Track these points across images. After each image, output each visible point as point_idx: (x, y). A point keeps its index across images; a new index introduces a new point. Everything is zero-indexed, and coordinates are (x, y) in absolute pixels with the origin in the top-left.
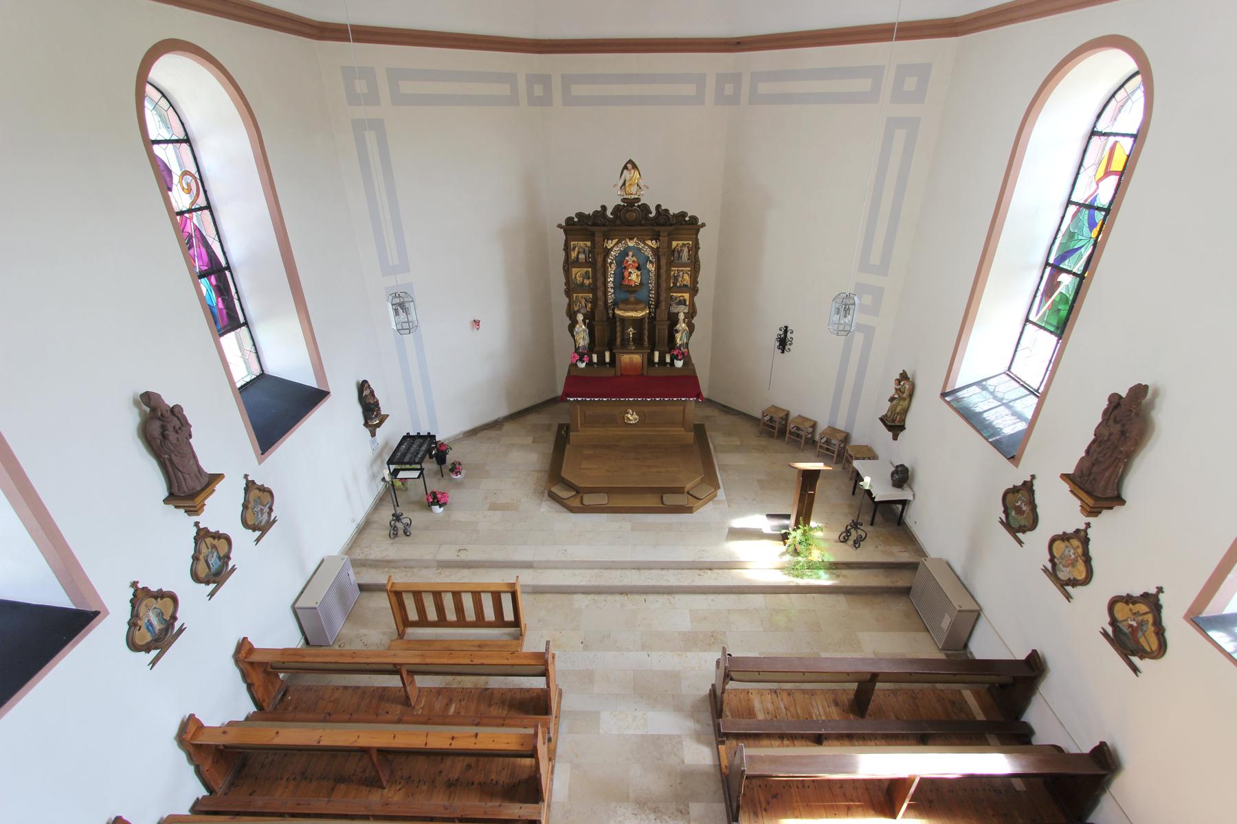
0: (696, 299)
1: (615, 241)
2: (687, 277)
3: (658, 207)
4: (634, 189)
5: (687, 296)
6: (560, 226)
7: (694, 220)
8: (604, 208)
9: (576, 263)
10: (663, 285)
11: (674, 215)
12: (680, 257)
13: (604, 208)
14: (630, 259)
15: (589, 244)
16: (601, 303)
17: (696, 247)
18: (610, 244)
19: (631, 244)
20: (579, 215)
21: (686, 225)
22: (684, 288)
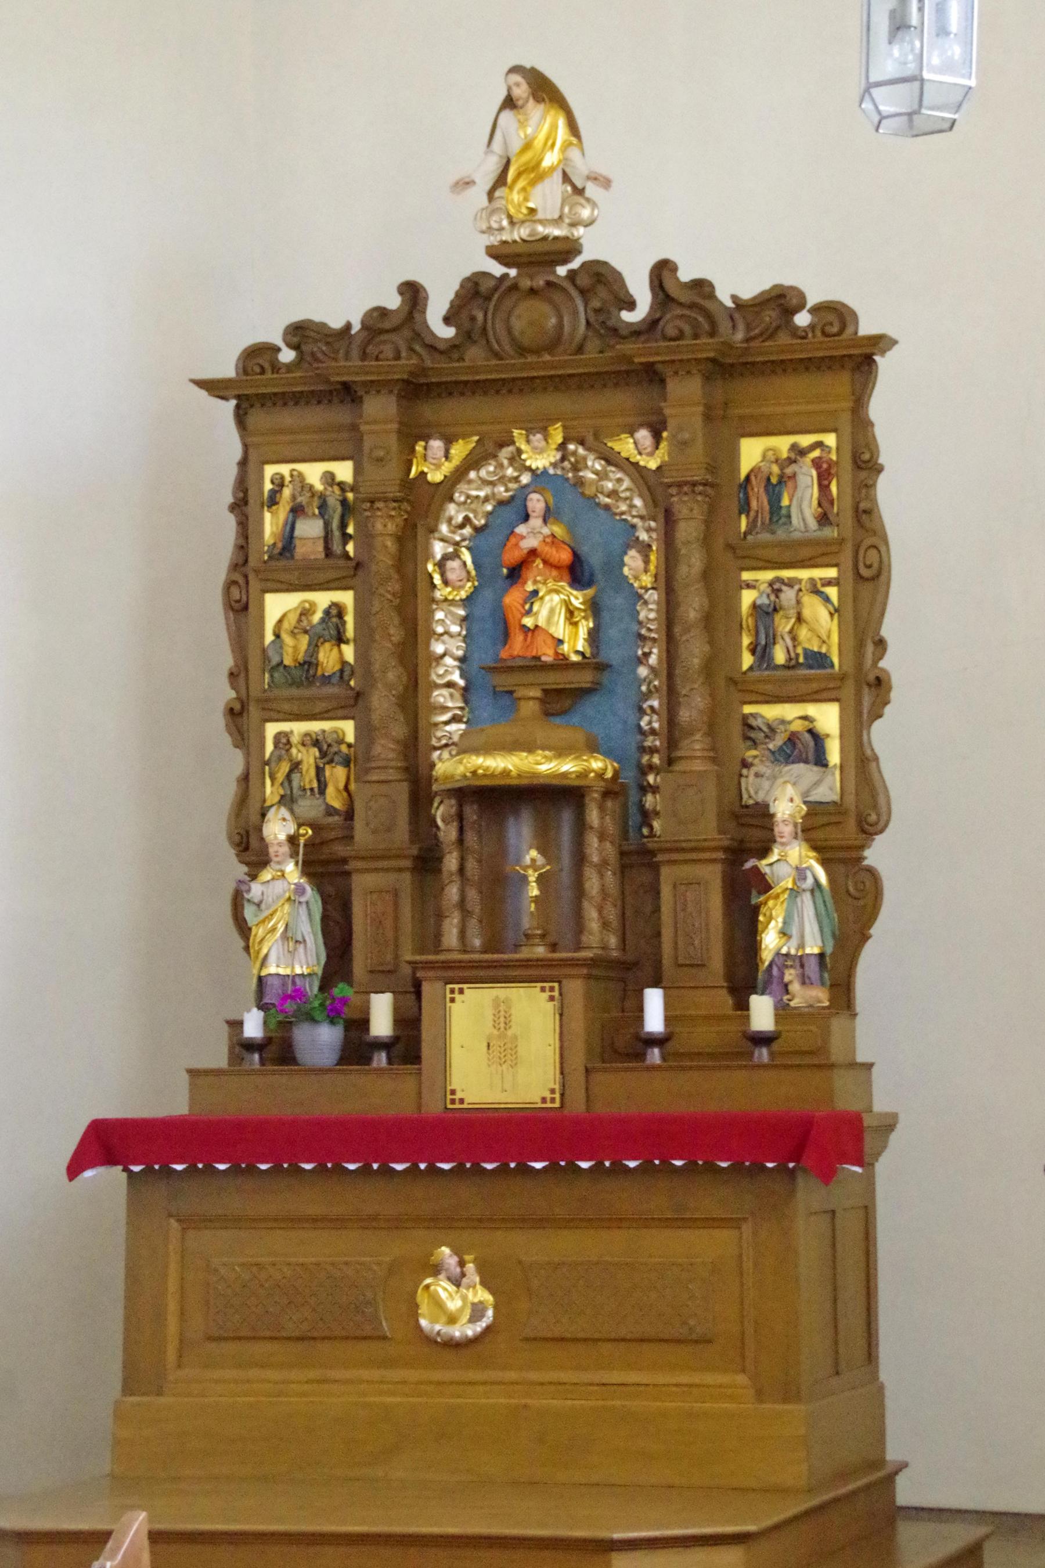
0: (881, 735)
1: (460, 450)
2: (818, 612)
3: (662, 272)
4: (547, 197)
5: (827, 717)
6: (214, 387)
7: (836, 316)
8: (413, 293)
9: (285, 567)
10: (694, 651)
11: (740, 304)
12: (777, 513)
13: (413, 293)
14: (532, 534)
15: (344, 471)
16: (386, 750)
17: (865, 463)
18: (434, 463)
19: (541, 456)
20: (300, 333)
21: (803, 355)
22: (810, 676)
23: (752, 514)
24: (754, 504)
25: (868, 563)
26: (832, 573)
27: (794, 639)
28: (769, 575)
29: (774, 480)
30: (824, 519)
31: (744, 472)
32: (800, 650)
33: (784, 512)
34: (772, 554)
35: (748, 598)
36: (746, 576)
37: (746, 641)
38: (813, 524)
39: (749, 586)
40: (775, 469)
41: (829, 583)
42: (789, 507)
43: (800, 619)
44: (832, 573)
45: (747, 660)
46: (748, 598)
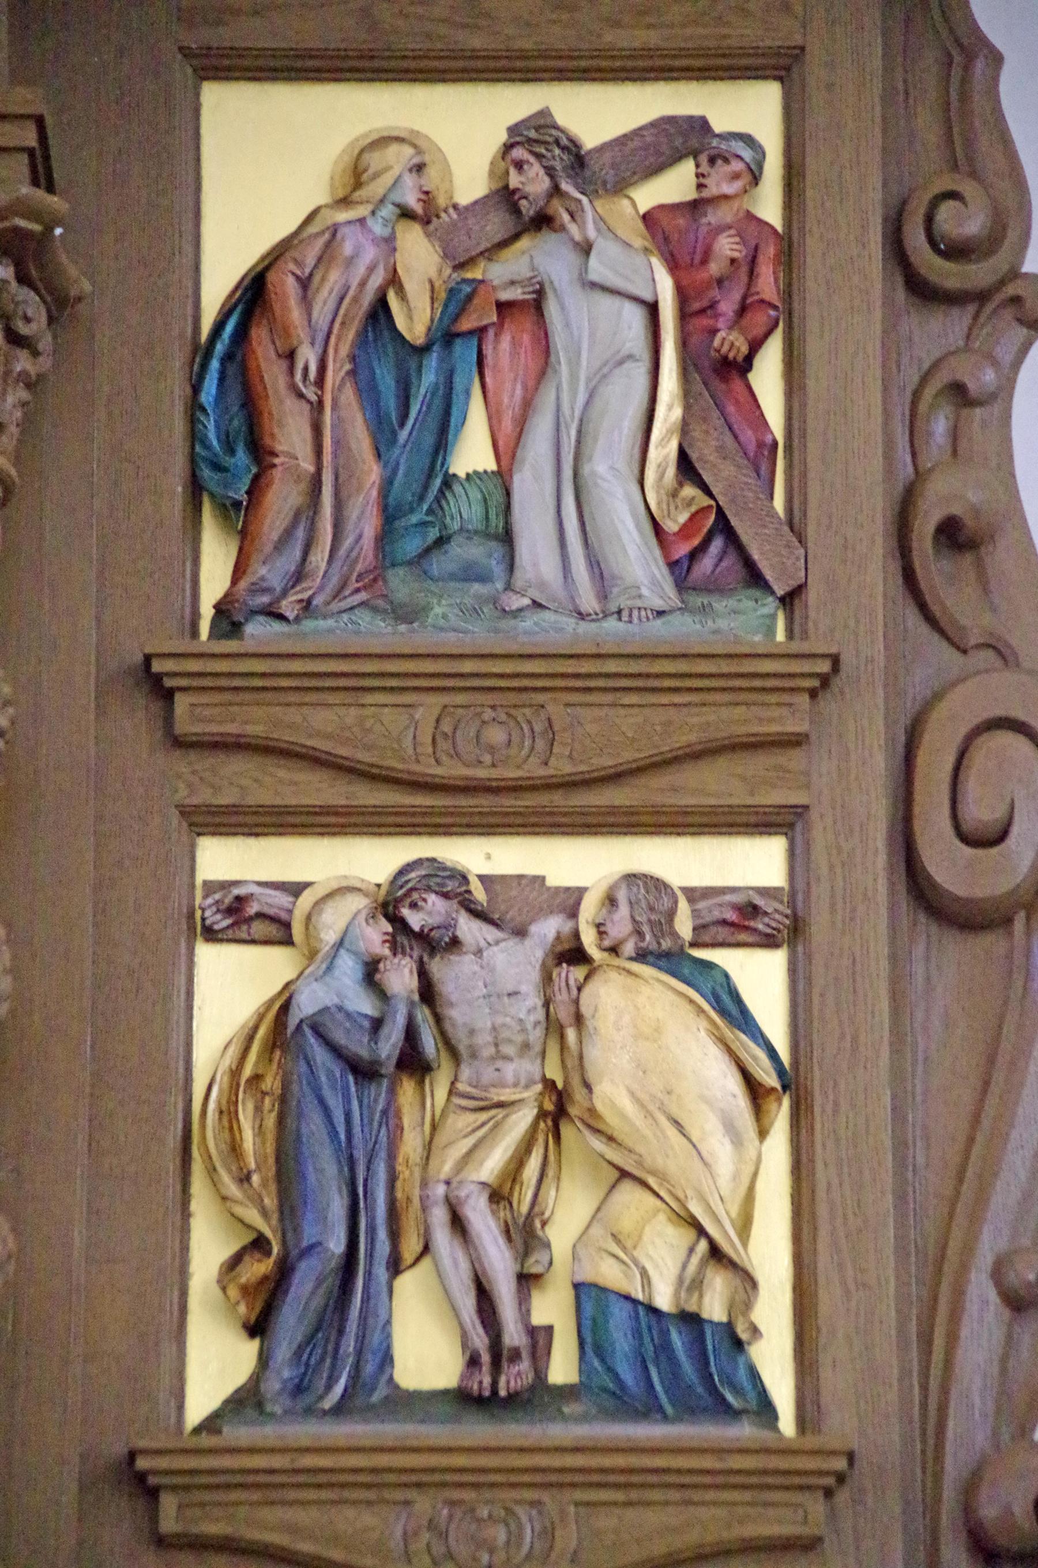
23: (282, 499)
24: (291, 435)
25: (980, 811)
26: (756, 863)
27: (526, 1235)
28: (375, 860)
29: (414, 319)
30: (710, 549)
31: (218, 282)
32: (552, 1307)
33: (466, 509)
34: (400, 730)
35: (229, 989)
36: (223, 860)
37: (209, 1248)
38: (640, 566)
39: (242, 918)
40: (420, 258)
41: (744, 920)
42: (502, 478)
43: (559, 1108)
44: (756, 863)
45: (215, 1362)
46: (229, 989)
